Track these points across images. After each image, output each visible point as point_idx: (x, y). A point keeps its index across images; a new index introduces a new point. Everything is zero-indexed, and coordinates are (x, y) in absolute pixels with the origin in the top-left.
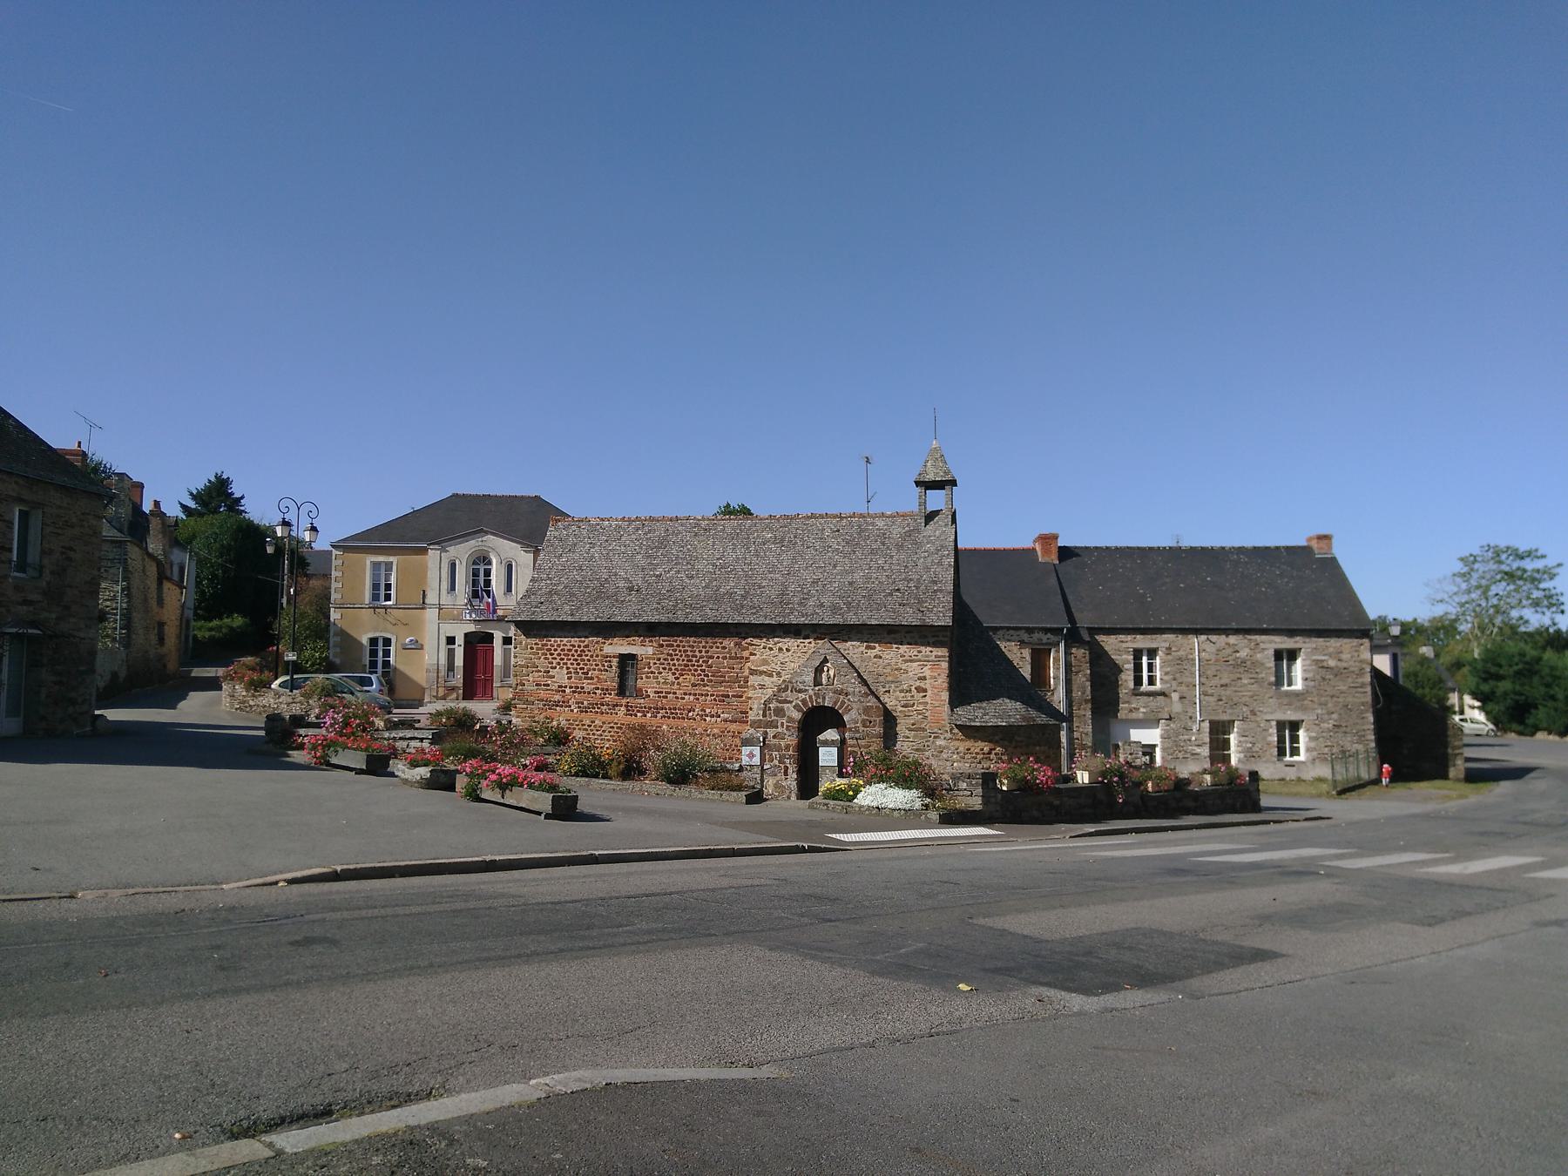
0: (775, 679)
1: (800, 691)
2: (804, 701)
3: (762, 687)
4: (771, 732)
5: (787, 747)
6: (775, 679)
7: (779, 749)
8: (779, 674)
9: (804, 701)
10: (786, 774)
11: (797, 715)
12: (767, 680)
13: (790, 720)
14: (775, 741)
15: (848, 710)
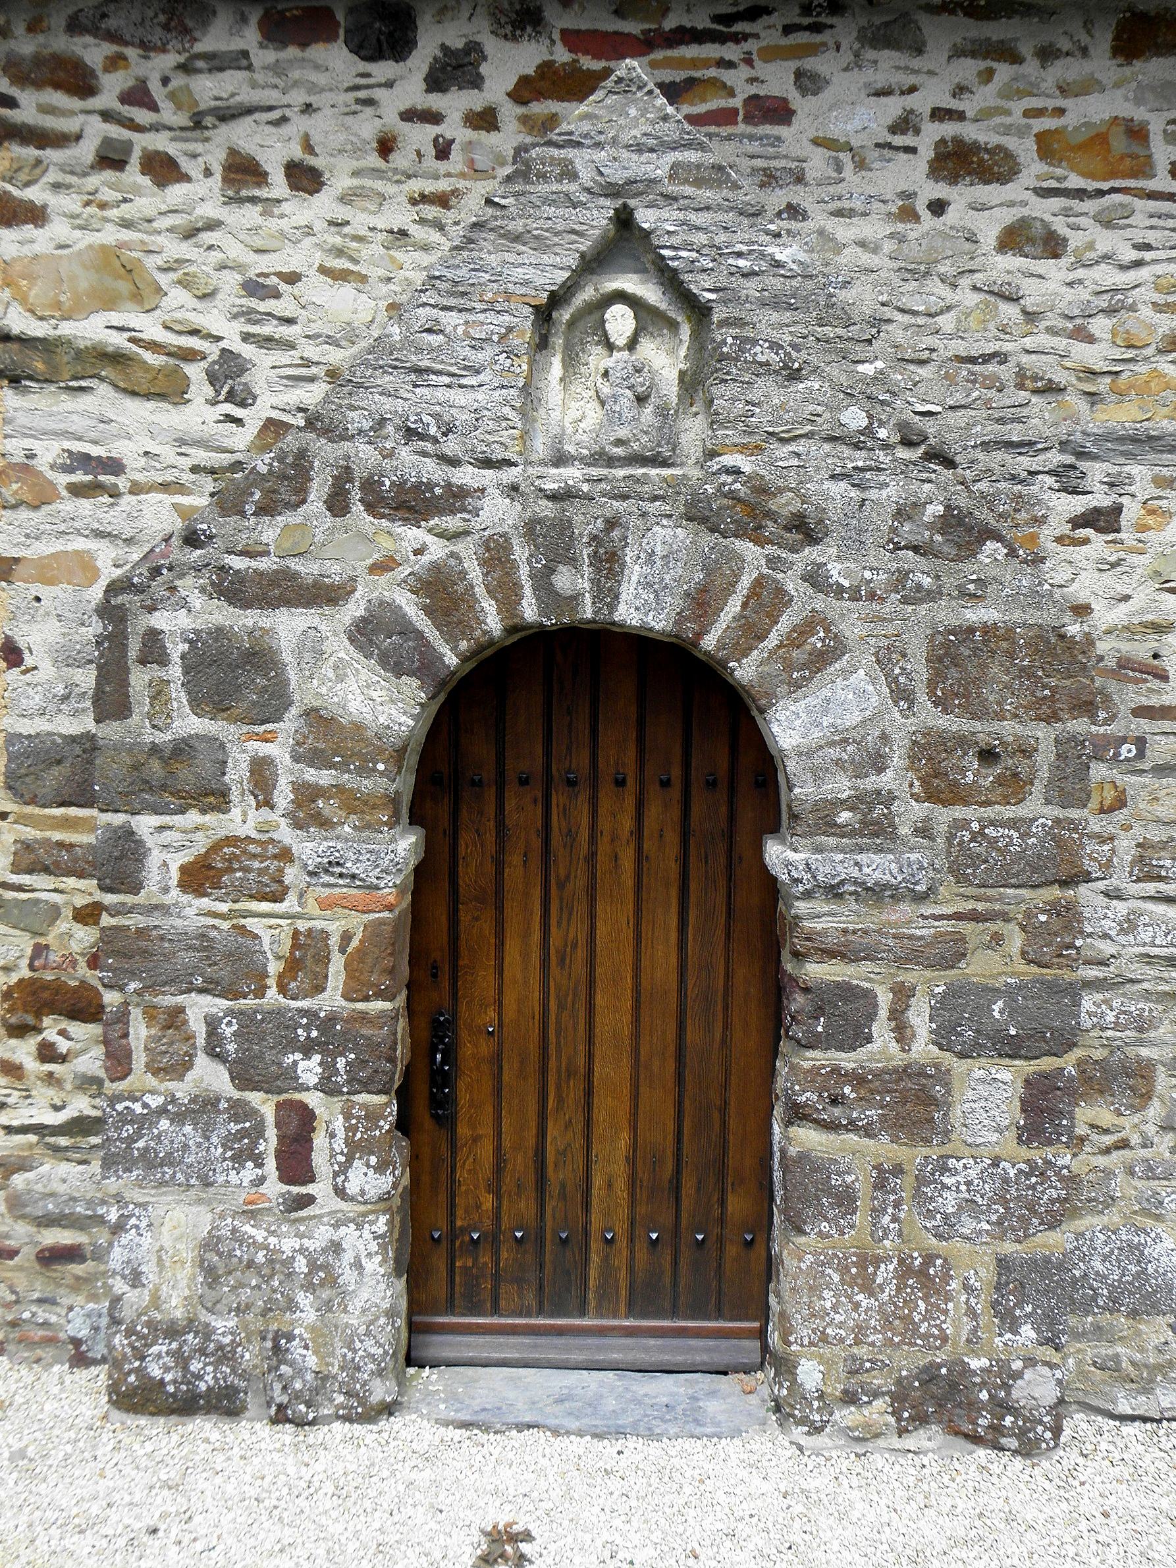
0: (199, 413)
1: (412, 503)
2: (441, 591)
3: (96, 475)
4: (169, 841)
5: (306, 958)
6: (199, 413)
7: (232, 970)
8: (229, 378)
9: (441, 591)
10: (295, 1164)
11: (388, 707)
12: (136, 430)
13: (328, 737)
14: (193, 912)
15: (816, 656)
